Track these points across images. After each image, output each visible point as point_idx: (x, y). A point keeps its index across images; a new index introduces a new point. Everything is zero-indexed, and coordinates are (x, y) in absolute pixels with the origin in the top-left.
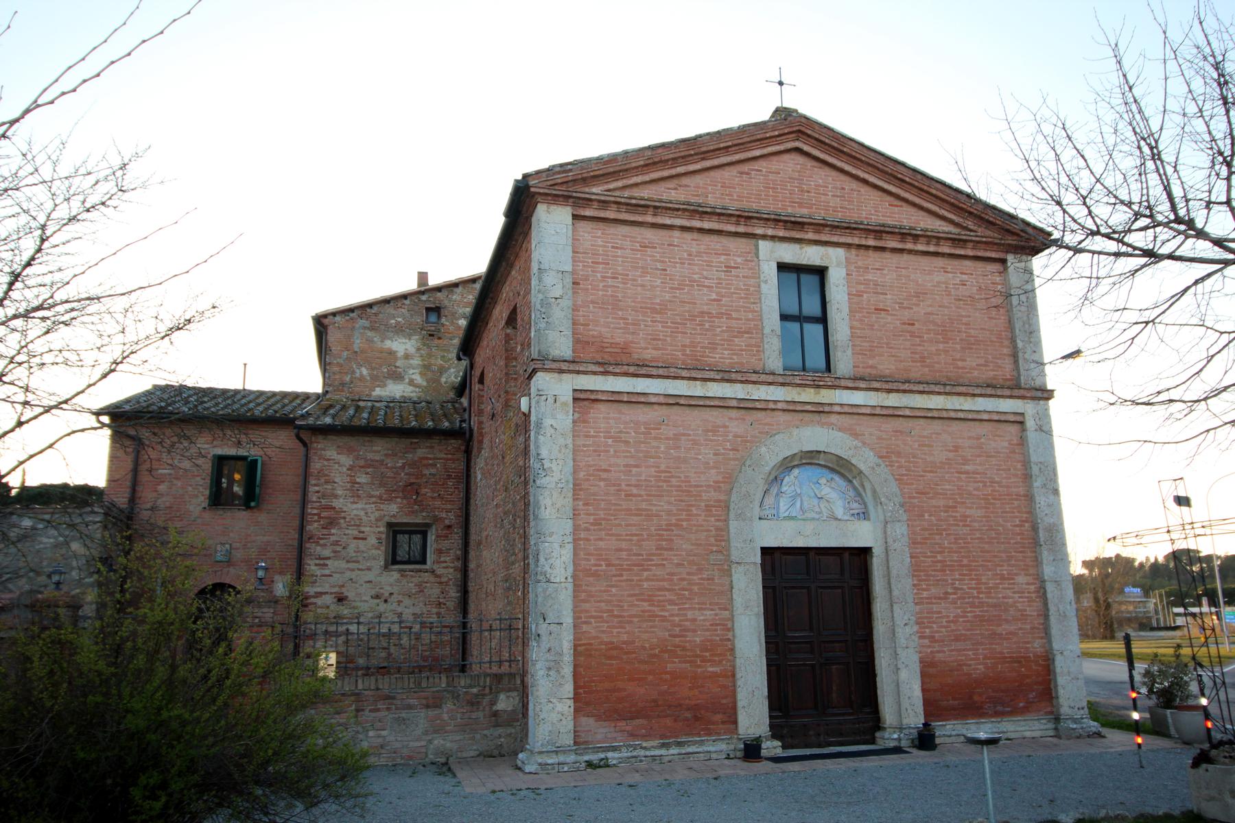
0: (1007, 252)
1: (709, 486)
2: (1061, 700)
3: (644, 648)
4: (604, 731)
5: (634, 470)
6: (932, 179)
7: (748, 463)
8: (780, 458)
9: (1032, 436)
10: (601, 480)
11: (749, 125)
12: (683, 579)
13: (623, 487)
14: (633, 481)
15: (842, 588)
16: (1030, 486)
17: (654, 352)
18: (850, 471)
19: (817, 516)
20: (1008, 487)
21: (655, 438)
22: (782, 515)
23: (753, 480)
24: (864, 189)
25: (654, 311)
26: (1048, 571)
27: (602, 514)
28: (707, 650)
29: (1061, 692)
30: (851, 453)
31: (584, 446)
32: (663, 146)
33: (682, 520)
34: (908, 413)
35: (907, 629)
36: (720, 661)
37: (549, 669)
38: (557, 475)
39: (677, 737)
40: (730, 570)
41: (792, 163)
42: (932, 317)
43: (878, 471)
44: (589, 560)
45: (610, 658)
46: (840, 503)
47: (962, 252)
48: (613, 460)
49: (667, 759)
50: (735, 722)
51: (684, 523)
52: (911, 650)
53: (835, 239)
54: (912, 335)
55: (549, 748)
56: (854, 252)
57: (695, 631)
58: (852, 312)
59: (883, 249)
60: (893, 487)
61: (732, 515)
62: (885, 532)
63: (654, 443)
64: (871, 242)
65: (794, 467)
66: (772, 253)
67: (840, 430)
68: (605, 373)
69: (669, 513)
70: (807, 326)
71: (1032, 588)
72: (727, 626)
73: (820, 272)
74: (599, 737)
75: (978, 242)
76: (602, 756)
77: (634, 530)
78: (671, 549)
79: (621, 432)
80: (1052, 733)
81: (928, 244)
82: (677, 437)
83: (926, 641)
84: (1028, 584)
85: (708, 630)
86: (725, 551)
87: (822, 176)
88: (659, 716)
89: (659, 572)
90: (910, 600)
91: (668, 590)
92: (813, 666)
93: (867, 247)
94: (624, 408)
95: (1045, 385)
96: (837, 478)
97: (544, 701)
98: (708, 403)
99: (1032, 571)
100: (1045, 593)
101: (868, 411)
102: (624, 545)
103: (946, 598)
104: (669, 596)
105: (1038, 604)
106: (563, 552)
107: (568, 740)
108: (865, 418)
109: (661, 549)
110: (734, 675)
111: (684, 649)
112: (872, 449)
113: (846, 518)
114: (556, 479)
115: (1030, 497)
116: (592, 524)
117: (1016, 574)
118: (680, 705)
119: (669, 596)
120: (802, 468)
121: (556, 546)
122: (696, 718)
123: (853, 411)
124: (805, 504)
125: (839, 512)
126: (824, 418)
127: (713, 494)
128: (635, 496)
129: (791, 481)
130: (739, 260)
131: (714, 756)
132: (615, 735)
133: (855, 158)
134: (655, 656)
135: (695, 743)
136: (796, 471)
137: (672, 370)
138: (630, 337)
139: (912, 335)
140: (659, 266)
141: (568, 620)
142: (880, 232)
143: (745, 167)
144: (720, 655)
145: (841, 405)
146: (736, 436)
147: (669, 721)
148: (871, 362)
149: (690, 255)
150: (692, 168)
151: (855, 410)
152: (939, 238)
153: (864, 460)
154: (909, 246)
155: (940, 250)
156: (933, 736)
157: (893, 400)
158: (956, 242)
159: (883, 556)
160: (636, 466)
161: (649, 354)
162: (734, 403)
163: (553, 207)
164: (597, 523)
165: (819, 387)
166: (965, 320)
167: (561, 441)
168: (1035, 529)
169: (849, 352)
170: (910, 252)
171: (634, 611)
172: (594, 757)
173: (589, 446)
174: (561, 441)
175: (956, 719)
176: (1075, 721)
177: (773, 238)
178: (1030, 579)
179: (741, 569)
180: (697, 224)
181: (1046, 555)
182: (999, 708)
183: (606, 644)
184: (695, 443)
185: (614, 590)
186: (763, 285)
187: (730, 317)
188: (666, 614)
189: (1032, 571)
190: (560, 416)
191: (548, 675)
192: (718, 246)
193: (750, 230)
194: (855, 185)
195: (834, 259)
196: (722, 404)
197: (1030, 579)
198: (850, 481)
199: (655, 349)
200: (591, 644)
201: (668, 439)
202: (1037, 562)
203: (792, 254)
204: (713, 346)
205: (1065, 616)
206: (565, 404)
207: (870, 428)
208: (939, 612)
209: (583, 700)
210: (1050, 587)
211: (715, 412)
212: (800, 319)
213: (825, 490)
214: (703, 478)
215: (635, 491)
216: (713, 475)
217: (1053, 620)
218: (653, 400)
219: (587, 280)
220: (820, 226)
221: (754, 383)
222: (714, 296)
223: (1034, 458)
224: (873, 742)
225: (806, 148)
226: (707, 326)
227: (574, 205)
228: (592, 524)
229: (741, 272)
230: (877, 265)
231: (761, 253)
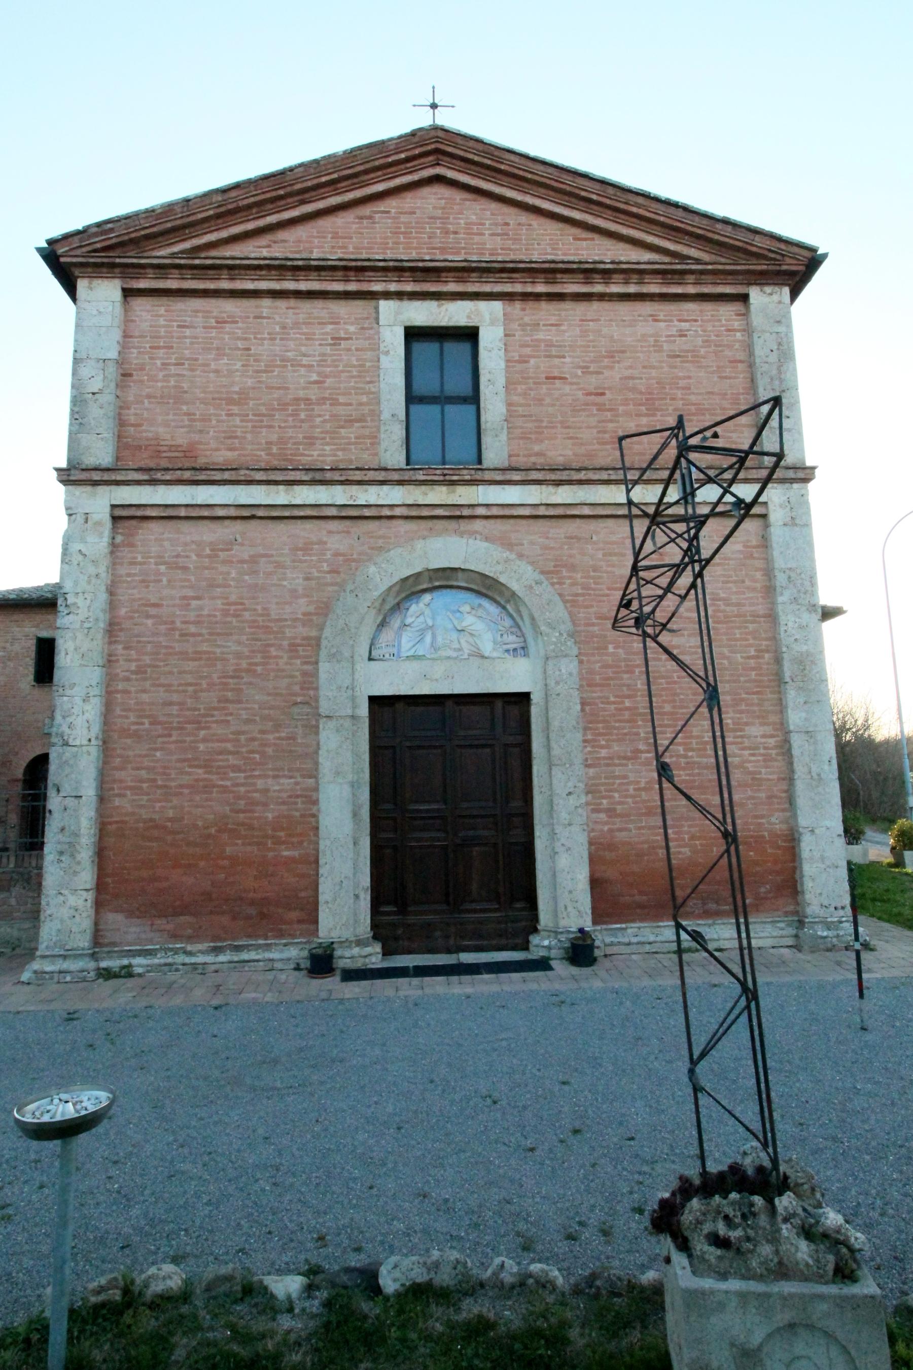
0: (749, 284)
1: (296, 620)
2: (808, 896)
3: (195, 826)
4: (138, 930)
5: (194, 603)
6: (629, 191)
7: (349, 587)
8: (396, 579)
9: (777, 533)
10: (148, 616)
11: (360, 148)
12: (253, 739)
13: (178, 624)
14: (192, 616)
15: (491, 746)
16: (774, 603)
17: (229, 454)
18: (501, 594)
19: (454, 654)
20: (738, 605)
21: (224, 562)
22: (404, 654)
23: (357, 611)
24: (537, 222)
25: (230, 401)
26: (795, 718)
27: (147, 659)
28: (283, 829)
29: (808, 884)
30: (500, 568)
31: (128, 575)
32: (237, 186)
33: (256, 664)
34: (586, 511)
35: (572, 801)
36: (301, 843)
37: (61, 853)
38: (83, 613)
39: (234, 939)
40: (317, 727)
41: (431, 200)
42: (631, 383)
43: (538, 590)
44: (127, 717)
45: (150, 839)
46: (488, 636)
47: (678, 290)
48: (166, 592)
49: (213, 967)
50: (316, 922)
51: (259, 669)
52: (575, 829)
53: (487, 288)
54: (601, 408)
55: (56, 951)
56: (518, 305)
57: (265, 805)
58: (509, 386)
59: (560, 297)
60: (560, 611)
61: (323, 654)
62: (545, 672)
63: (224, 569)
64: (541, 288)
65: (424, 591)
66: (395, 317)
67: (487, 539)
68: (153, 482)
69: (238, 655)
70: (449, 409)
71: (772, 741)
72: (311, 799)
73: (470, 335)
74: (130, 938)
75: (702, 272)
76: (125, 962)
77: (189, 678)
78: (239, 702)
79: (178, 556)
80: (790, 942)
81: (627, 283)
82: (254, 560)
83: (603, 816)
84: (764, 736)
85: (283, 803)
86: (312, 703)
87: (476, 212)
88: (211, 913)
89: (220, 730)
90: (578, 760)
91: (230, 753)
92: (445, 848)
93: (537, 297)
94: (185, 526)
95: (804, 463)
96: (486, 603)
97: (52, 892)
98: (297, 513)
99: (773, 718)
100: (789, 750)
101: (527, 512)
102: (175, 697)
103: (635, 758)
104: (232, 760)
105: (779, 764)
106: (88, 707)
107: (83, 942)
108: (524, 522)
109: (227, 701)
110: (317, 861)
111: (251, 828)
112: (532, 563)
113: (495, 654)
114: (81, 617)
115: (772, 617)
116: (132, 672)
117: (747, 724)
118: (241, 899)
119: (232, 760)
120: (436, 594)
121: (78, 700)
122: (263, 916)
123: (505, 514)
124: (439, 639)
125: (487, 648)
126: (464, 525)
127: (302, 631)
128: (193, 635)
129: (421, 610)
130: (352, 329)
131: (279, 965)
132: (152, 934)
133: (514, 176)
134: (209, 836)
135: (258, 947)
136: (427, 597)
137: (242, 472)
138: (196, 437)
139: (601, 408)
140: (240, 344)
141: (89, 791)
142: (551, 271)
143: (366, 210)
144: (301, 835)
145: (487, 506)
146: (337, 554)
147: (225, 920)
148: (537, 448)
149: (284, 328)
150: (287, 215)
151: (507, 512)
152: (641, 272)
153: (518, 576)
154: (599, 288)
155: (645, 289)
156: (591, 947)
157: (564, 495)
158: (663, 274)
159: (542, 703)
160: (198, 598)
161: (222, 456)
162: (333, 512)
163: (96, 282)
164: (140, 671)
165: (453, 483)
166: (682, 383)
167: (92, 570)
168: (778, 660)
169: (504, 437)
170: (602, 297)
171: (186, 780)
172: (114, 963)
173: (135, 575)
174: (92, 570)
175: (642, 920)
176: (828, 926)
177: (400, 295)
178: (769, 730)
179: (332, 724)
180: (290, 285)
181: (792, 695)
182: (712, 906)
183: (145, 821)
184: (279, 565)
185: (158, 754)
186: (383, 358)
187: (335, 403)
188: (228, 783)
189: (773, 718)
190: (91, 539)
191: (59, 861)
192: (324, 314)
193: (365, 287)
194: (524, 217)
195: (487, 317)
196: (316, 515)
197: (769, 730)
198: (504, 608)
199: (230, 450)
200: (122, 822)
201: (242, 562)
202: (781, 707)
203: (424, 314)
204: (310, 441)
205: (820, 778)
206: (99, 523)
207: (531, 536)
208: (625, 777)
209: (105, 894)
210: (797, 741)
211: (309, 525)
212: (441, 399)
213: (469, 621)
214: (288, 609)
215: (193, 629)
216: (302, 606)
217: (800, 786)
218: (221, 513)
219: (142, 369)
220: (464, 271)
221: (360, 483)
222: (315, 377)
223: (779, 562)
224: (525, 947)
225: (450, 174)
226: (303, 416)
227: (123, 277)
228: (132, 672)
229: (353, 344)
230: (553, 320)
231: (381, 317)
